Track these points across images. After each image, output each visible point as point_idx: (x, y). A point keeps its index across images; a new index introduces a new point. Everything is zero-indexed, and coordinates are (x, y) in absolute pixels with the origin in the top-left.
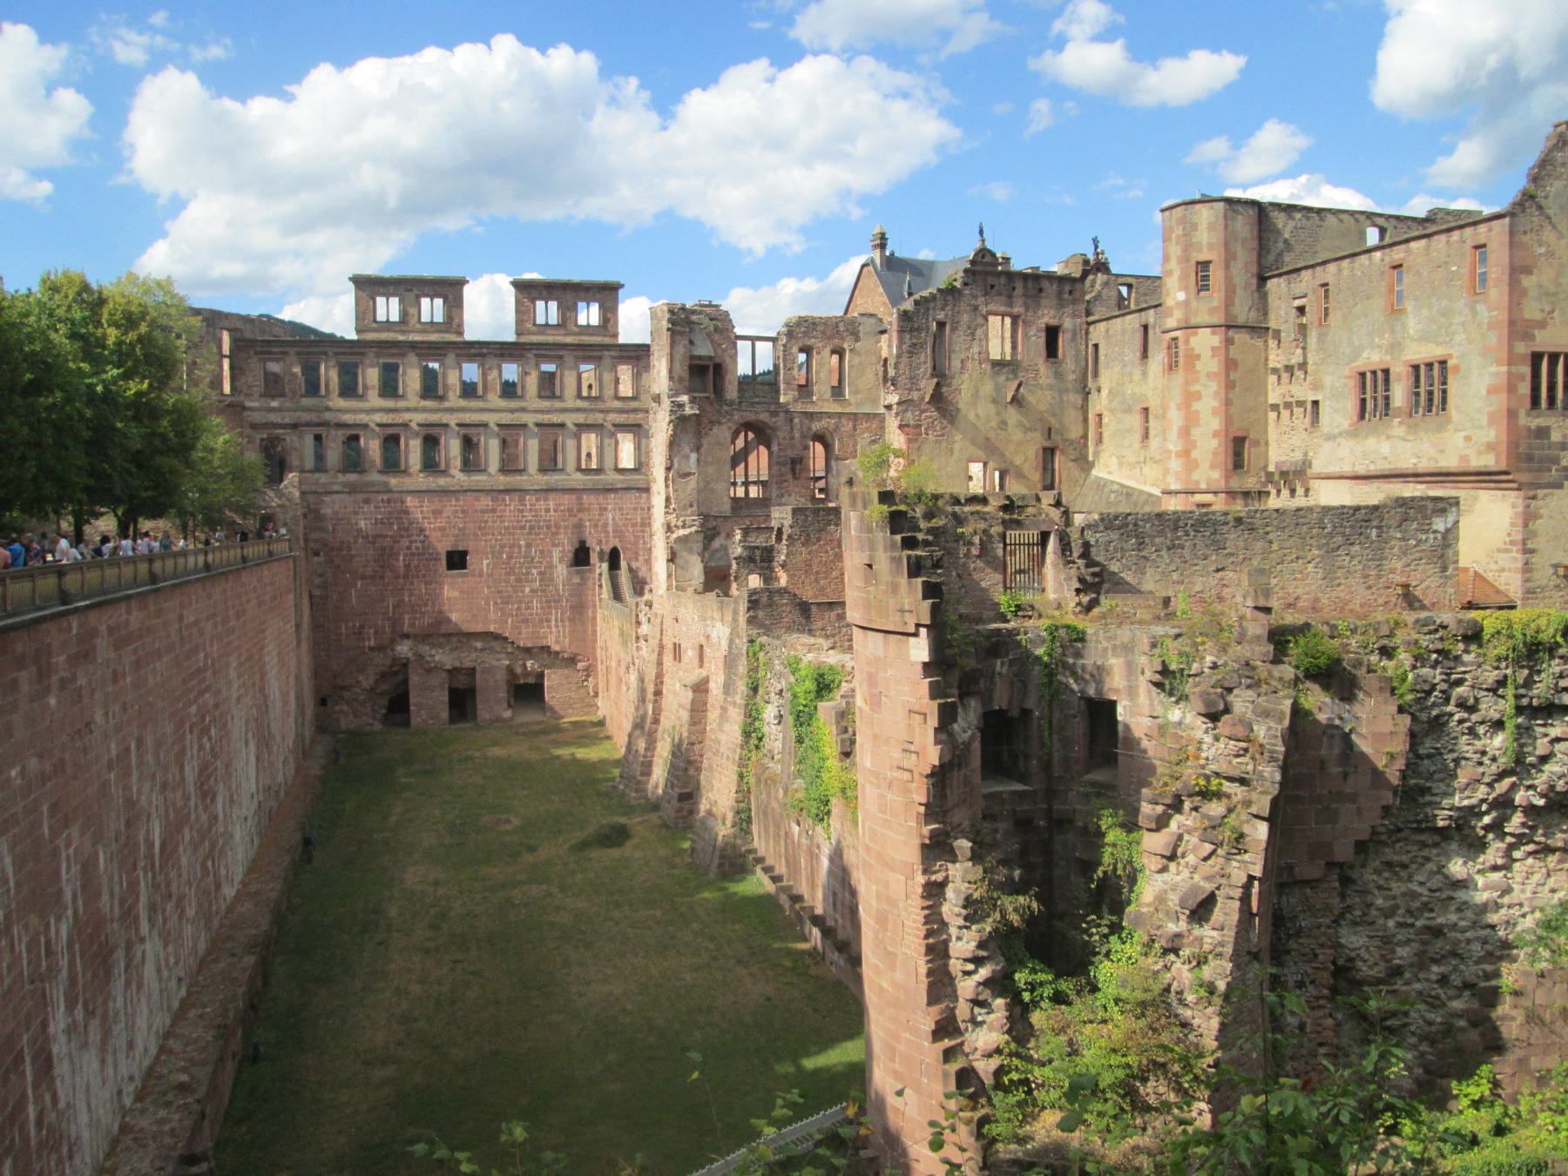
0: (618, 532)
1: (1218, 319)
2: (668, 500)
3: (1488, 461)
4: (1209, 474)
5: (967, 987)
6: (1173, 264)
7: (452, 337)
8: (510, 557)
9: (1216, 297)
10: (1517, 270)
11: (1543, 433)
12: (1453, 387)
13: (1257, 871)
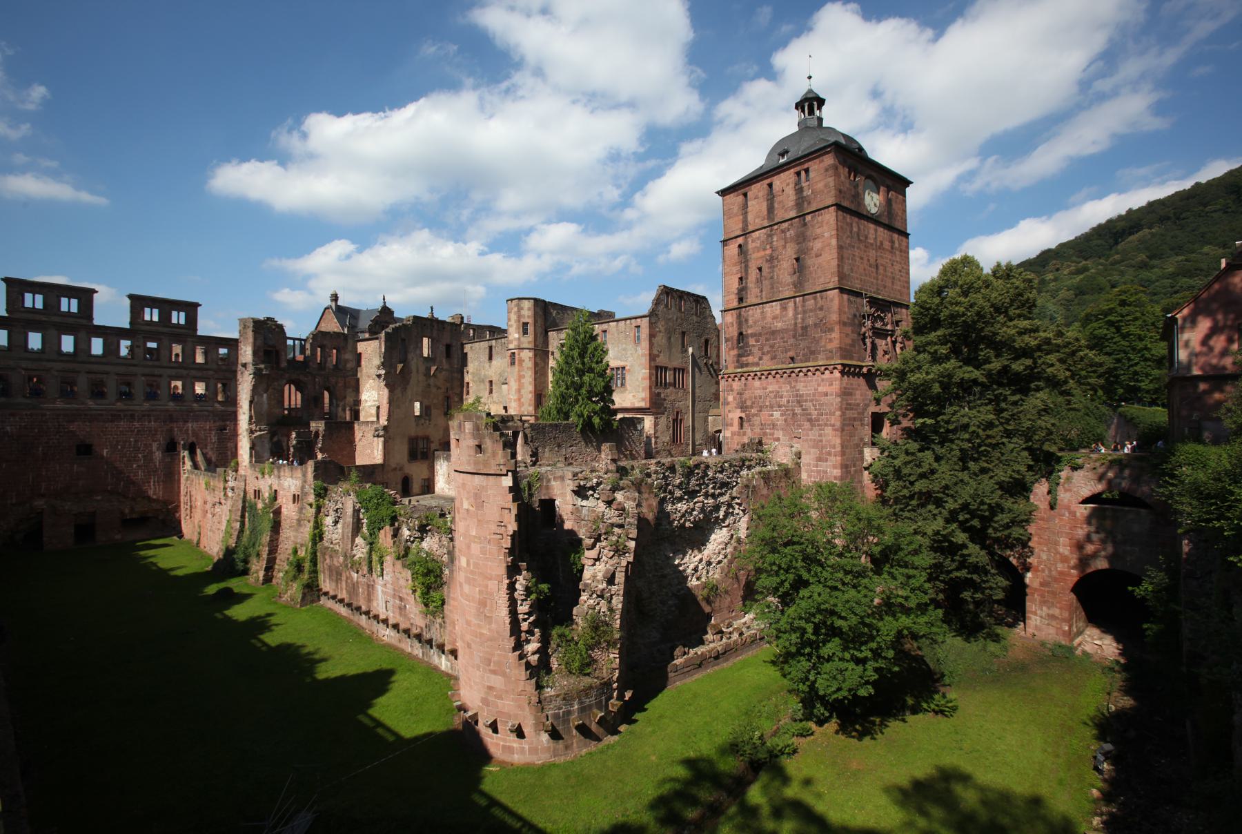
0: (195, 434)
1: (531, 346)
2: (251, 418)
3: (642, 405)
4: (528, 408)
5: (524, 626)
6: (512, 322)
7: (84, 322)
8: (123, 447)
9: (530, 337)
10: (652, 336)
11: (659, 394)
12: (628, 377)
13: (631, 559)
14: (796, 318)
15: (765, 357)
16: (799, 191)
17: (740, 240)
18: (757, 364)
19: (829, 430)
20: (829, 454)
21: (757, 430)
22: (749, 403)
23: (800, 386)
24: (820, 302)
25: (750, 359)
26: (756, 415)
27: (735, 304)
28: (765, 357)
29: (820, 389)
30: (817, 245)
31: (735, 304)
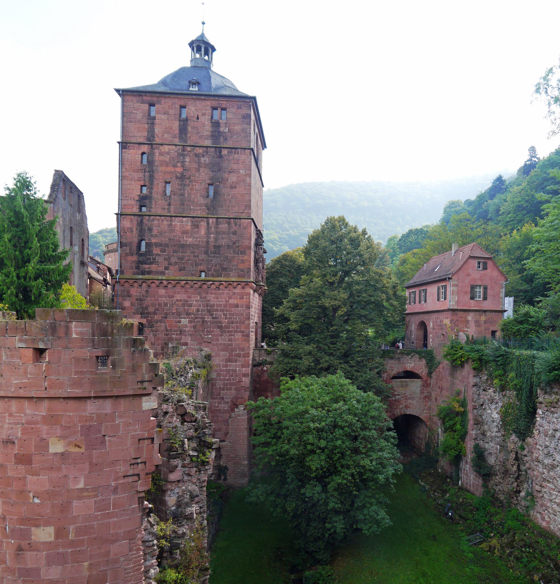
14: (208, 237)
15: (171, 267)
16: (216, 124)
17: (145, 148)
18: (163, 273)
19: (238, 336)
20: (239, 355)
21: (161, 335)
22: (151, 309)
23: (211, 298)
24: (234, 228)
25: (154, 267)
26: (161, 321)
27: (135, 210)
28: (171, 267)
29: (231, 301)
30: (233, 178)
31: (135, 210)
